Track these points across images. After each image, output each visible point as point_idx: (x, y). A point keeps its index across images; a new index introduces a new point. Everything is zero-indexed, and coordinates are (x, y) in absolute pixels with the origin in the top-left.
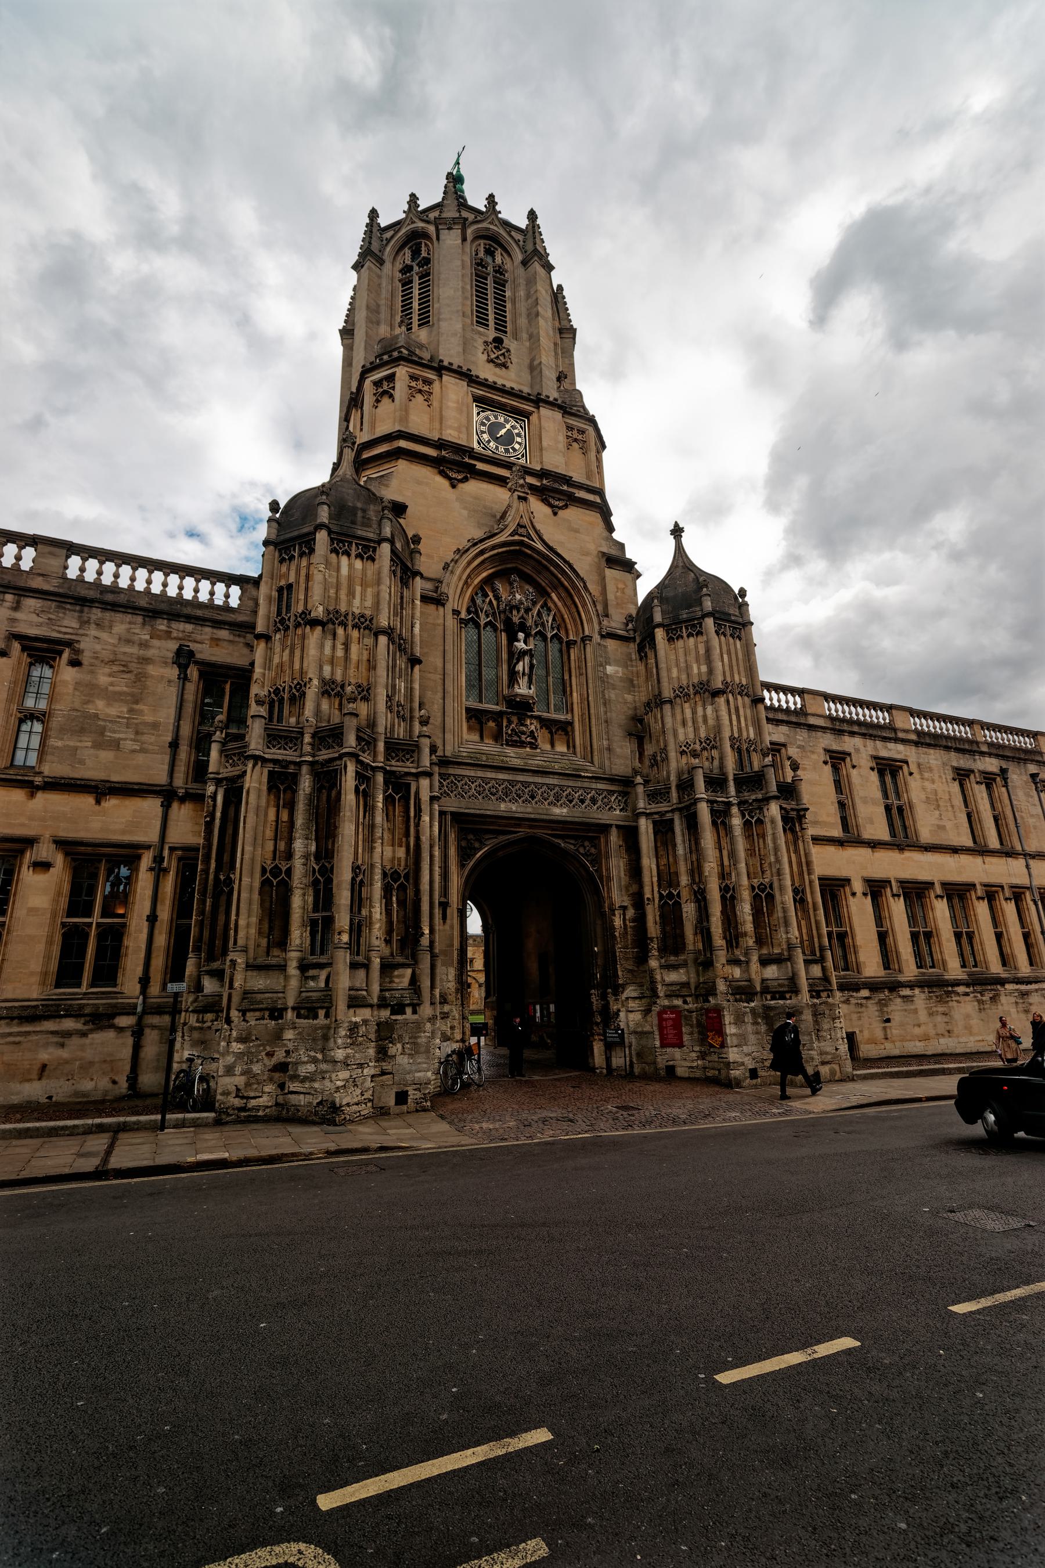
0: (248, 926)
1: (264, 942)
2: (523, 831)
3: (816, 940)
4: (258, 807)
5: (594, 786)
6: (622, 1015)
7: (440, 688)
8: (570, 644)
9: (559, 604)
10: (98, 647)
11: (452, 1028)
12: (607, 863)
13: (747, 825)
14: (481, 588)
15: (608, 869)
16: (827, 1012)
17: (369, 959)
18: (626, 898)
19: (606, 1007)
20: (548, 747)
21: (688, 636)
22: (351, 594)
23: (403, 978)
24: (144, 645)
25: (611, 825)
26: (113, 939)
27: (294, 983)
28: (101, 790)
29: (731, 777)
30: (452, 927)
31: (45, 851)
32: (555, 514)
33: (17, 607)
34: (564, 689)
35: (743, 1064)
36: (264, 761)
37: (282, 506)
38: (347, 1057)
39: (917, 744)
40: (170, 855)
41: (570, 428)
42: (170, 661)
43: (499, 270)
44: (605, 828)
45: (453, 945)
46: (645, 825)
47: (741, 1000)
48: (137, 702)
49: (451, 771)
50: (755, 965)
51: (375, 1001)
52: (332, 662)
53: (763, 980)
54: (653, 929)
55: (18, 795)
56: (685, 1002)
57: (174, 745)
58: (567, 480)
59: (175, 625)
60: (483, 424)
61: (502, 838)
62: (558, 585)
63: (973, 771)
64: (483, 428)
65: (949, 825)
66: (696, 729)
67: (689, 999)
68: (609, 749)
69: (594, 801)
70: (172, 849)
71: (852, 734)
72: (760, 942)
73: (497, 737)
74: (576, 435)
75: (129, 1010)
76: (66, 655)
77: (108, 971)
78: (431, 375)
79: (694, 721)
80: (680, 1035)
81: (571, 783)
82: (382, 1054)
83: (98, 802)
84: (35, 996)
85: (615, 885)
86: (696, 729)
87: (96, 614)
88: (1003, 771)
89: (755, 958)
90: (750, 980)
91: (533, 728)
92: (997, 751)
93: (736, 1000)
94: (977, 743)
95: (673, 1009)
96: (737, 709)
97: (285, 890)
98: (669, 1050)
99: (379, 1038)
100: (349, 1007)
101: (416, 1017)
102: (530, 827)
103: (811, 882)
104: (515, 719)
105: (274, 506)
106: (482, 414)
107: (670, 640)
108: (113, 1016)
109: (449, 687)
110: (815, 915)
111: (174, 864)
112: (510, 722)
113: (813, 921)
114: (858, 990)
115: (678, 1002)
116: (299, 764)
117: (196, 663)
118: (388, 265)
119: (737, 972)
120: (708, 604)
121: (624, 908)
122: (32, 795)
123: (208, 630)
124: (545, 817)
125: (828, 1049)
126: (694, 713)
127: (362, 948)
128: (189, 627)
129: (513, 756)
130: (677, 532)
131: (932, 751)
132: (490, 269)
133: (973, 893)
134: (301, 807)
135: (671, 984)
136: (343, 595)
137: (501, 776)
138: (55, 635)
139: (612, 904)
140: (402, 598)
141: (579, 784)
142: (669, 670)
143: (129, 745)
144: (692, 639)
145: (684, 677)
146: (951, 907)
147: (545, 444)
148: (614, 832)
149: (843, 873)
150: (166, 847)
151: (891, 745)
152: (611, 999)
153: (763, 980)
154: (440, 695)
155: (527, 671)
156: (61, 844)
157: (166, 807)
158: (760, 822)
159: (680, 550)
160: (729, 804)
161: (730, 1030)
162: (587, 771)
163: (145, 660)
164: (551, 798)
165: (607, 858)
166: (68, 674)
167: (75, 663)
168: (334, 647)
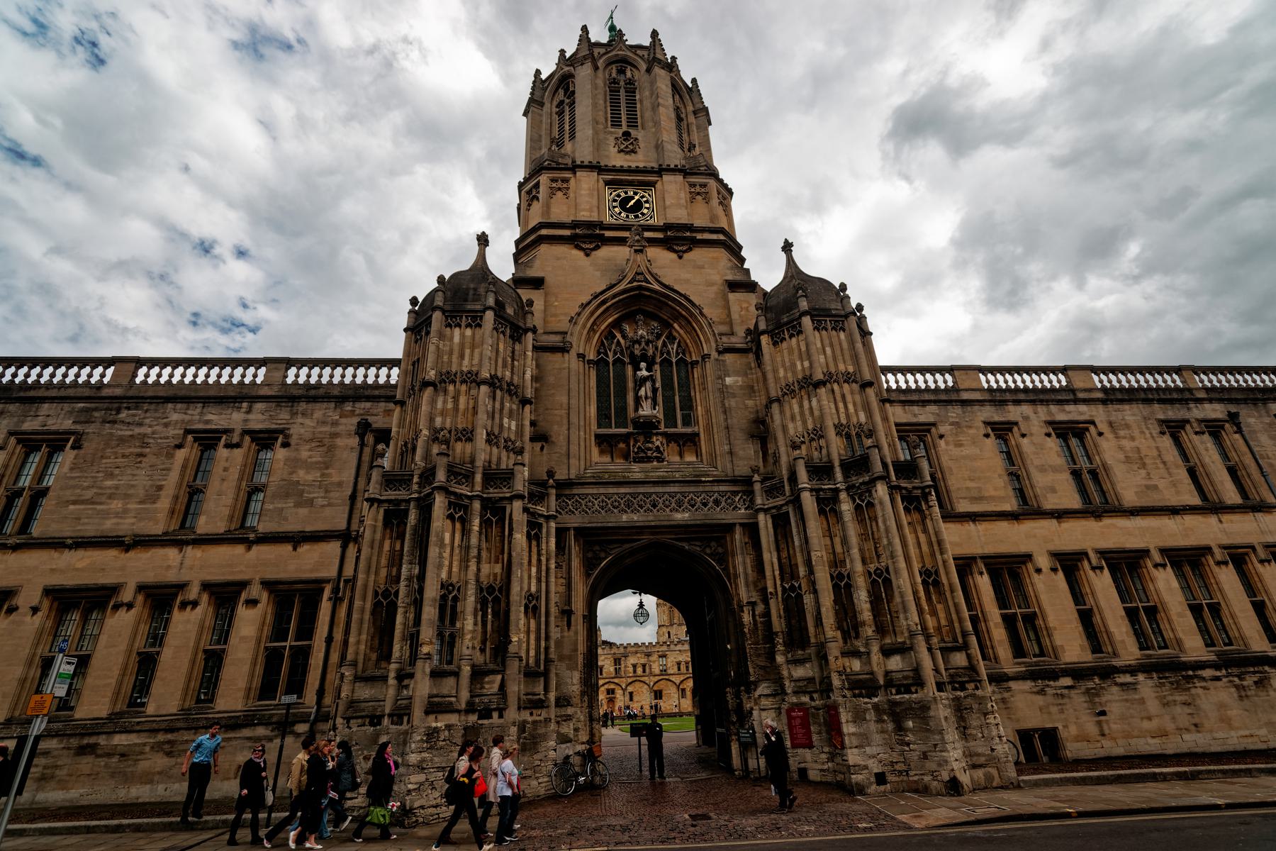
0: (358, 642)
1: (374, 656)
2: (646, 538)
3: (956, 625)
4: (373, 542)
5: (716, 489)
6: (755, 713)
7: (565, 421)
9: (682, 332)
10: (302, 431)
11: (576, 730)
12: (734, 561)
13: (858, 508)
15: (734, 567)
16: (975, 706)
17: (459, 667)
18: (754, 594)
19: (740, 705)
20: (677, 459)
21: (791, 337)
22: (462, 356)
24: (335, 424)
25: (734, 524)
26: (301, 656)
27: (391, 692)
28: (297, 539)
29: (837, 463)
30: (576, 633)
31: (255, 591)
32: (680, 257)
33: (249, 411)
34: (688, 404)
35: (866, 767)
36: (380, 502)
37: (420, 300)
38: (423, 760)
39: (1104, 402)
40: (345, 587)
41: (692, 185)
43: (630, 82)
44: (730, 528)
45: (576, 650)
46: (764, 521)
47: (861, 695)
48: (327, 468)
49: (575, 491)
50: (876, 657)
51: (463, 706)
52: (443, 413)
53: (887, 673)
54: (778, 624)
55: (240, 549)
56: (812, 699)
58: (690, 228)
59: (358, 405)
60: (615, 201)
61: (627, 546)
62: (677, 317)
63: (1188, 421)
65: (1162, 484)
66: (804, 422)
67: (815, 696)
68: (731, 453)
69: (717, 502)
71: (1017, 402)
72: (881, 630)
73: (626, 457)
74: (698, 189)
75: (304, 718)
76: (280, 441)
77: (296, 686)
78: (567, 175)
79: (802, 413)
80: (808, 734)
81: (692, 489)
83: (295, 549)
84: (240, 708)
86: (804, 422)
87: (303, 406)
88: (1233, 417)
89: (875, 648)
90: (872, 673)
91: (658, 443)
92: (1216, 394)
93: (855, 696)
94: (1190, 390)
95: (800, 706)
96: (843, 396)
97: (393, 608)
98: (800, 751)
100: (427, 713)
101: (501, 721)
102: (653, 534)
103: (944, 562)
104: (641, 438)
105: (414, 301)
107: (775, 344)
108: (294, 723)
109: (574, 419)
110: (953, 598)
112: (636, 441)
113: (950, 603)
114: (1056, 678)
115: (805, 699)
116: (408, 501)
117: (372, 431)
118: (547, 105)
119: (856, 665)
120: (804, 304)
121: (753, 604)
122: (249, 549)
123: (382, 404)
125: (980, 750)
126: (801, 406)
127: (456, 658)
128: (368, 405)
129: (637, 471)
130: (787, 247)
131: (1127, 407)
132: (622, 83)
133: (1209, 558)
135: (799, 680)
136: (455, 359)
137: (622, 490)
138: (274, 426)
139: (740, 601)
140: (513, 352)
141: (701, 489)
142: (775, 371)
143: (320, 502)
144: (794, 340)
145: (789, 375)
146: (1180, 575)
147: (668, 203)
148: (738, 530)
149: (1023, 549)
151: (1071, 408)
152: (744, 697)
153: (887, 673)
154: (565, 427)
155: (649, 394)
157: (344, 548)
158: (871, 505)
159: (791, 262)
160: (837, 491)
161: (848, 729)
162: (708, 476)
163: (334, 435)
165: (733, 556)
166: (281, 453)
167: (286, 445)
168: (445, 402)
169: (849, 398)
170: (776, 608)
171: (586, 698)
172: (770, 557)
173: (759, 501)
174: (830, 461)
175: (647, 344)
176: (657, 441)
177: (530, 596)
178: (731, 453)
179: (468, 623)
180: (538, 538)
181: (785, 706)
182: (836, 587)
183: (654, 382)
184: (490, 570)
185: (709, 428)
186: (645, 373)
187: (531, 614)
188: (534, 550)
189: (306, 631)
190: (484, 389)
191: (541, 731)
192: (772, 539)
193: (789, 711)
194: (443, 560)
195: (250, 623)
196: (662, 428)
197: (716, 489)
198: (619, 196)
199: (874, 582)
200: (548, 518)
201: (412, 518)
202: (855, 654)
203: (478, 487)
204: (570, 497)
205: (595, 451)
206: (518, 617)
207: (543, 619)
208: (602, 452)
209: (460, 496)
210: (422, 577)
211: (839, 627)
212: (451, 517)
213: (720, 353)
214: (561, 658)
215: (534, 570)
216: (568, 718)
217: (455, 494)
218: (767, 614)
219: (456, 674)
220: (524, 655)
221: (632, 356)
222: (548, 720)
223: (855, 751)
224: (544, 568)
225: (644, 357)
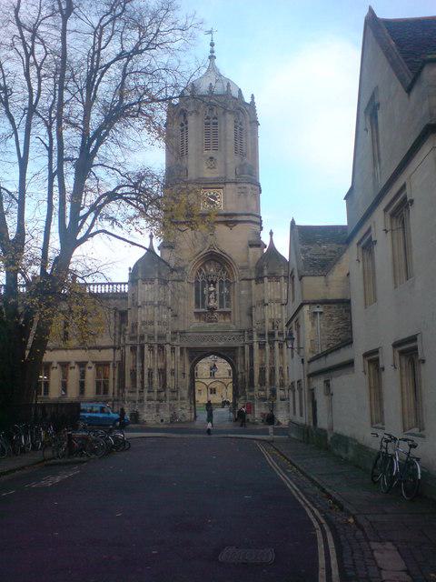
14: (200, 271)
28: (100, 348)
44: (236, 348)
46: (247, 347)
54: (247, 380)
58: (236, 215)
74: (243, 190)
75: (110, 400)
77: (106, 391)
82: (157, 411)
105: (130, 269)
119: (262, 393)
120: (266, 273)
130: (271, 233)
170: (247, 375)
172: (247, 359)
179: (156, 379)
182: (260, 371)
184: (160, 365)
185: (234, 310)
186: (212, 289)
190: (156, 308)
194: (148, 363)
195: (90, 374)
196: (219, 310)
202: (263, 390)
205: (194, 317)
208: (197, 318)
210: (143, 366)
211: (259, 382)
225: (212, 282)
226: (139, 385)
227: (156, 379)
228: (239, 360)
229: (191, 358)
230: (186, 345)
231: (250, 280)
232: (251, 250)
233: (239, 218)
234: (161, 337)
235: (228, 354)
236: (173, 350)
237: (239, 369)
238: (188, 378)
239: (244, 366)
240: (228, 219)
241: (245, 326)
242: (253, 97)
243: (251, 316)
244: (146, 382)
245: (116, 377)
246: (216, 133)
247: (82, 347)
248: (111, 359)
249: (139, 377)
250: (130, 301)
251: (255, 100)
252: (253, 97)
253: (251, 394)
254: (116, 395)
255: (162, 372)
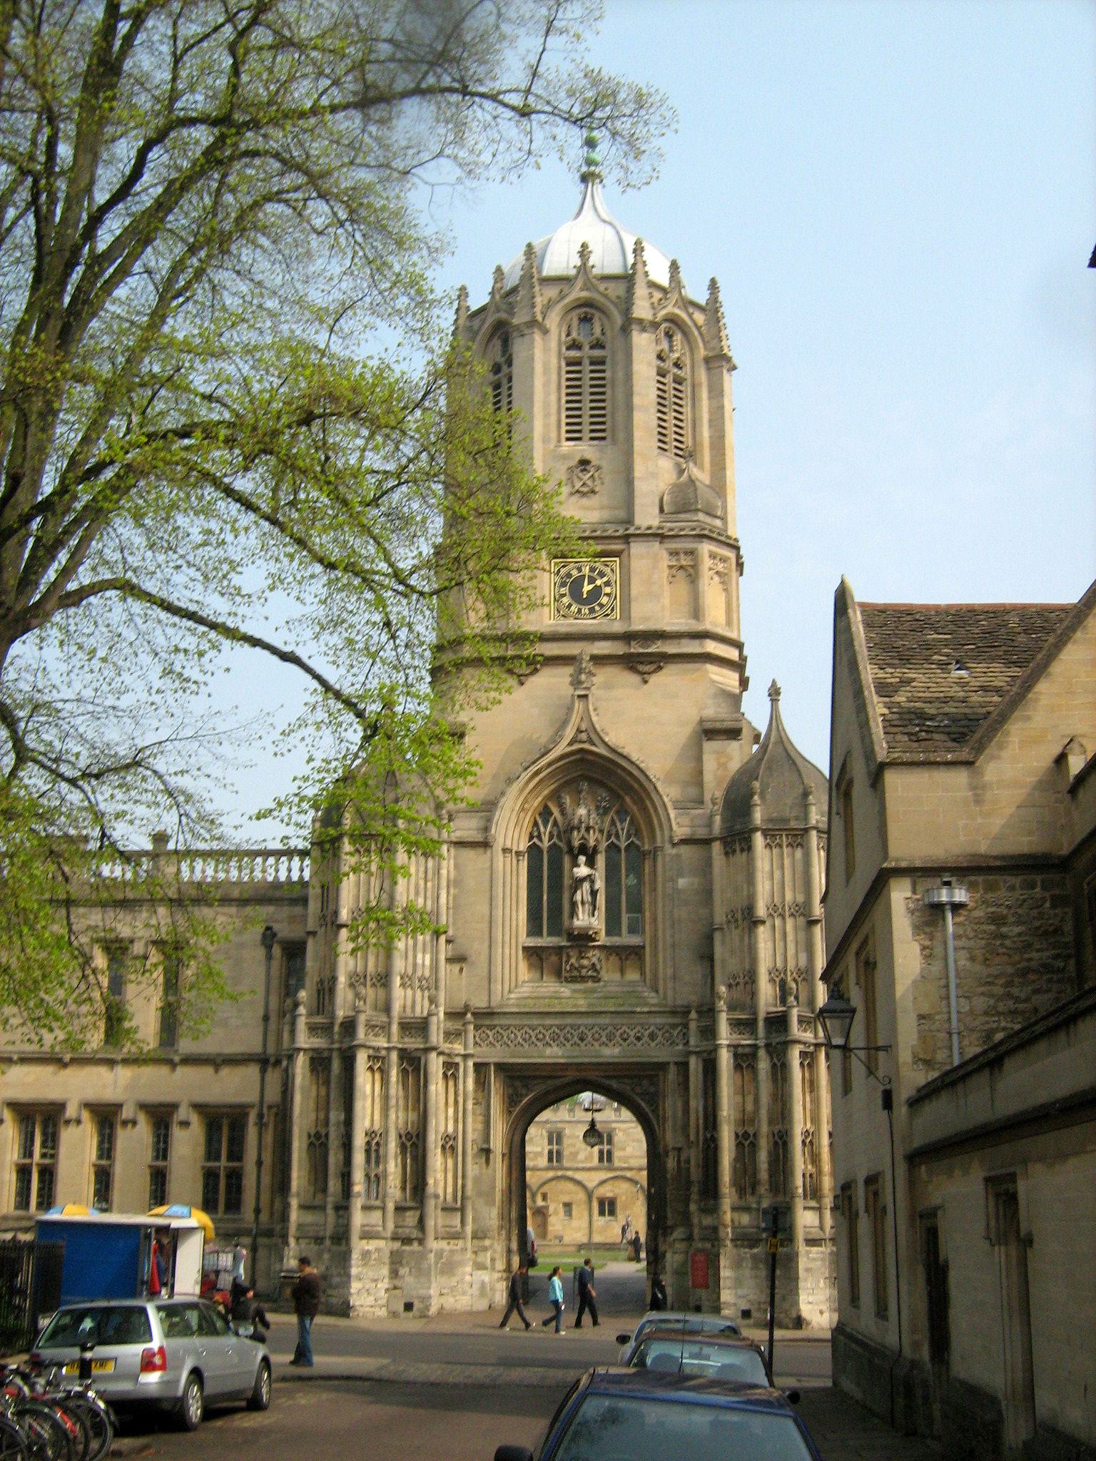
6: (668, 1255)
8: (644, 854)
9: (635, 808)
11: (493, 1260)
13: (774, 1066)
15: (664, 1109)
20: (617, 976)
23: (411, 1218)
26: (235, 1177)
34: (636, 906)
41: (674, 553)
42: (259, 942)
44: (662, 1066)
46: (694, 1064)
47: (742, 1246)
49: (496, 1022)
51: (389, 1234)
54: (696, 1174)
55: (164, 1070)
57: (266, 1018)
60: (563, 585)
61: (550, 1082)
62: (630, 789)
64: (563, 590)
69: (652, 1037)
70: (270, 1107)
73: (558, 974)
75: (247, 1232)
81: (625, 1021)
82: (394, 1274)
83: (217, 1071)
85: (669, 1124)
91: (594, 960)
95: (703, 1250)
99: (392, 1263)
100: (362, 1238)
106: (563, 571)
107: (727, 854)
111: (272, 1118)
112: (569, 957)
116: (331, 1050)
120: (758, 816)
121: (679, 1150)
123: (286, 909)
124: (594, 1060)
128: (271, 909)
130: (774, 693)
134: (333, 1085)
135: (706, 1228)
137: (548, 1022)
139: (666, 1146)
140: (426, 872)
144: (745, 854)
150: (265, 1106)
152: (661, 1239)
154: (486, 944)
155: (588, 898)
156: (197, 1107)
157: (263, 1071)
159: (775, 717)
162: (646, 1005)
164: (604, 1039)
169: (790, 937)
170: (694, 1156)
171: (504, 1232)
172: (696, 1104)
173: (692, 1041)
174: (755, 1013)
175: (588, 829)
176: (594, 956)
177: (447, 1137)
178: (674, 977)
180: (455, 1077)
181: (692, 1251)
182: (739, 1145)
183: (592, 882)
186: (583, 871)
187: (448, 1154)
188: (451, 1090)
189: (236, 1153)
191: (457, 1257)
192: (700, 1085)
193: (694, 1255)
194: (366, 1115)
196: (603, 939)
197: (652, 1020)
198: (569, 575)
199: (776, 1143)
200: (465, 1057)
201: (336, 1065)
202: (746, 1209)
203: (395, 1037)
204: (491, 1027)
205: (523, 966)
206: (437, 1162)
207: (460, 1158)
209: (377, 1049)
211: (735, 1183)
212: (371, 1068)
213: (674, 845)
214: (480, 1194)
215: (451, 1111)
216: (485, 1249)
217: (374, 1048)
218: (688, 1161)
219: (383, 1209)
220: (441, 1192)
221: (571, 849)
222: (464, 1250)
223: (728, 1292)
224: (461, 1109)
225: (583, 849)
226: (334, 1185)
227: (393, 1168)
228: (671, 1105)
229: (511, 1101)
230: (494, 1054)
231: (706, 842)
232: (711, 748)
233: (671, 648)
234: (419, 1027)
235: (632, 1085)
236: (451, 1069)
237: (670, 1138)
238: (499, 1167)
239: (685, 1127)
240: (636, 648)
241: (687, 994)
242: (713, 285)
243: (711, 959)
244: (358, 1176)
245: (268, 1158)
246: (599, 387)
247: (167, 1054)
248: (251, 1096)
249: (334, 1159)
250: (314, 906)
251: (721, 297)
252: (713, 285)
253: (708, 1221)
254: (264, 1217)
255: (415, 1144)
